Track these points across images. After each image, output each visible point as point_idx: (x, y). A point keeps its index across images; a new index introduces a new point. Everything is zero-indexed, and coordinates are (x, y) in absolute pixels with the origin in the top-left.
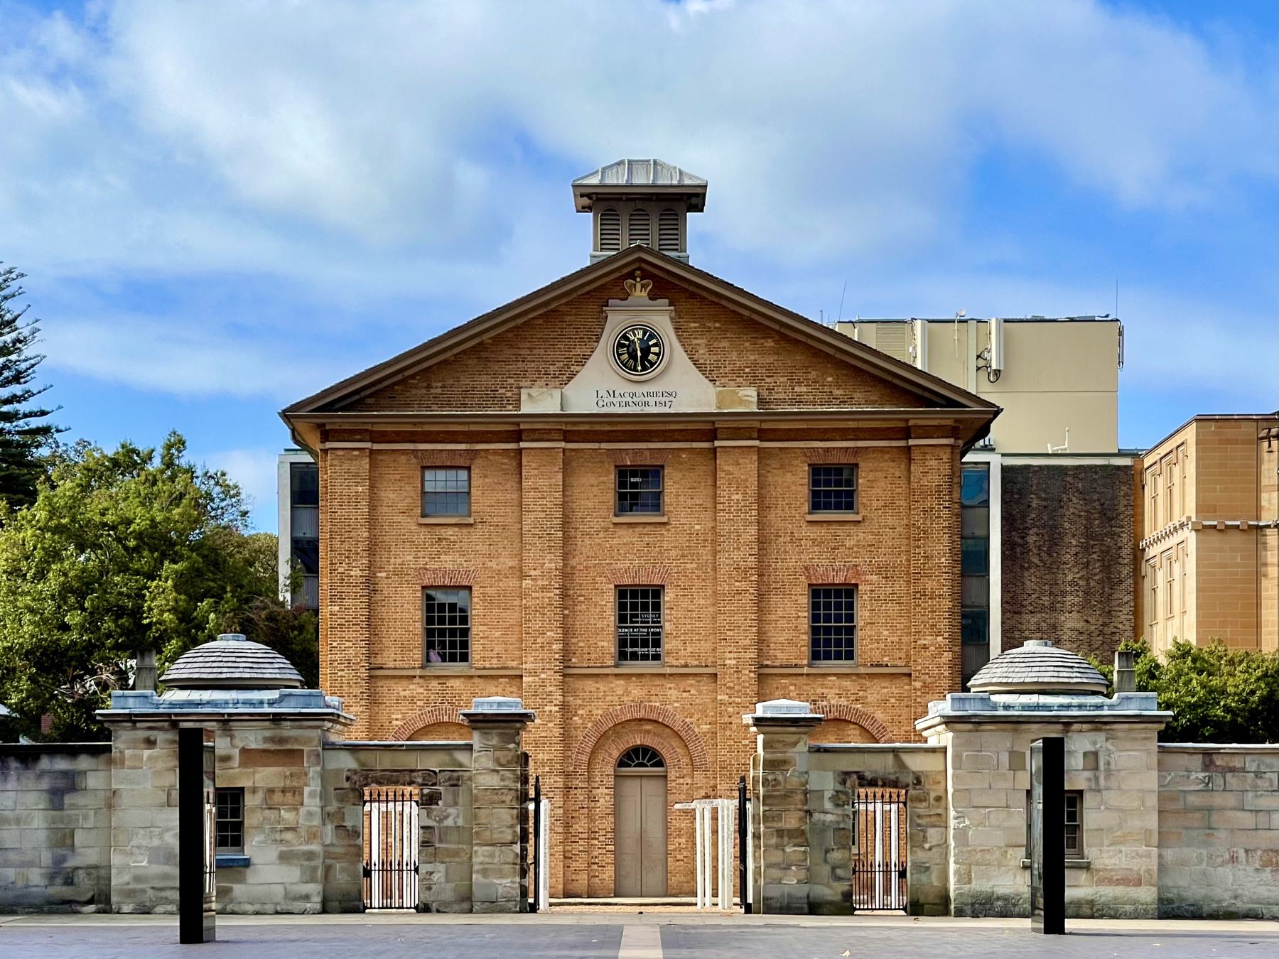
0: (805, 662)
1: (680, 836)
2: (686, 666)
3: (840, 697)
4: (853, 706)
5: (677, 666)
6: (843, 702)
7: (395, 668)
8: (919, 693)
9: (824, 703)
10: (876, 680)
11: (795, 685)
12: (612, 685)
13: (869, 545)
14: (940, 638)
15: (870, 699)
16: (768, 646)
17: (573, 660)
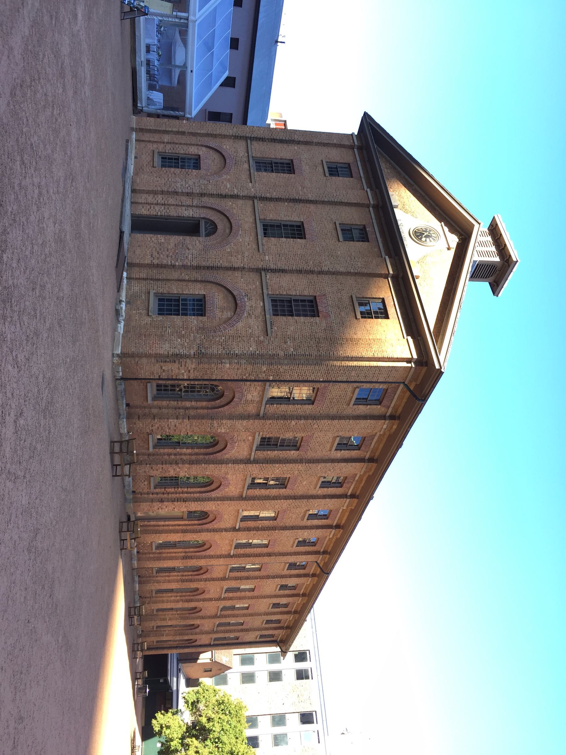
0: (270, 293)
1: (165, 240)
2: (263, 245)
3: (250, 307)
4: (246, 312)
5: (262, 241)
6: (247, 308)
7: (251, 149)
8: (256, 339)
9: (246, 300)
10: (262, 323)
11: (256, 287)
12: (249, 217)
13: (343, 323)
14: (292, 350)
15: (250, 320)
16: (277, 278)
17: (262, 205)
